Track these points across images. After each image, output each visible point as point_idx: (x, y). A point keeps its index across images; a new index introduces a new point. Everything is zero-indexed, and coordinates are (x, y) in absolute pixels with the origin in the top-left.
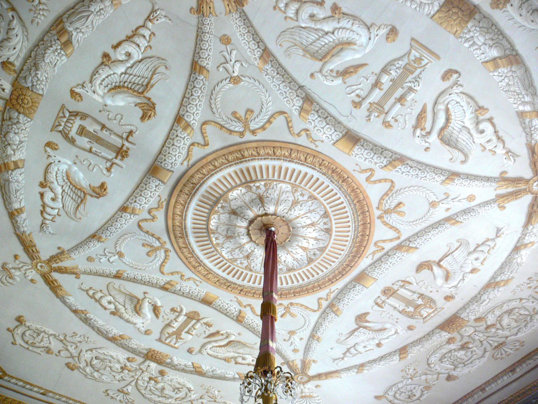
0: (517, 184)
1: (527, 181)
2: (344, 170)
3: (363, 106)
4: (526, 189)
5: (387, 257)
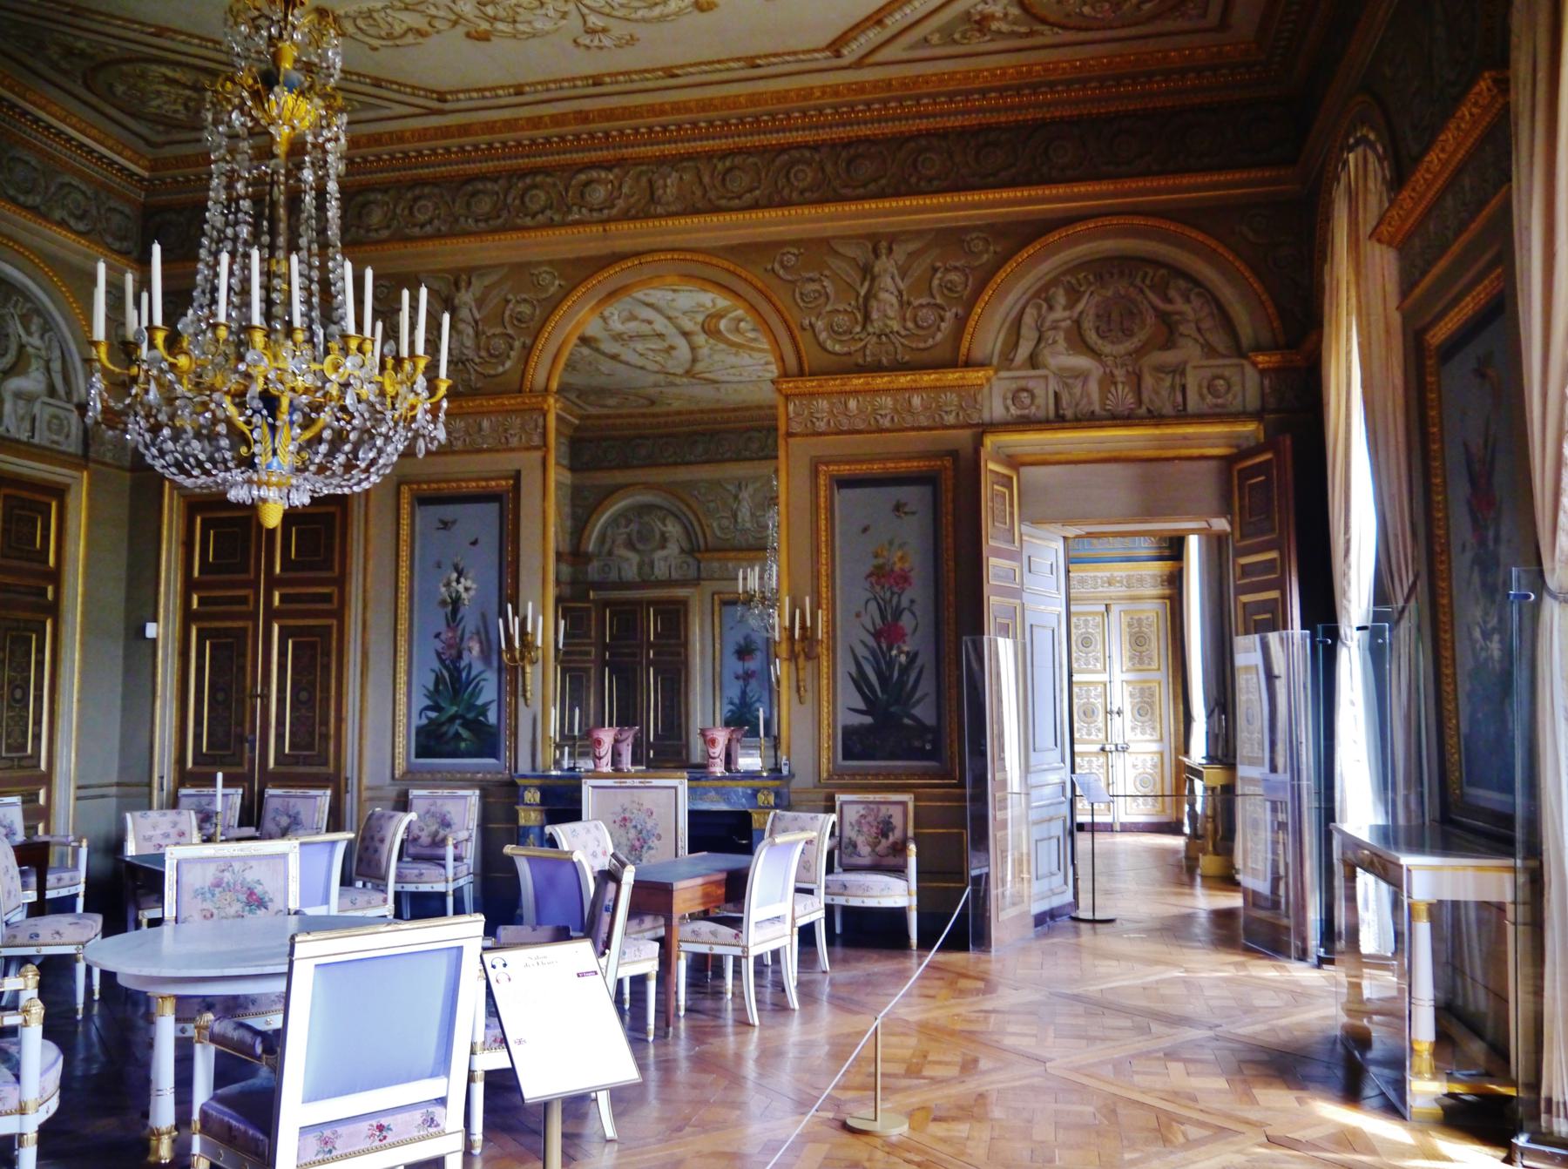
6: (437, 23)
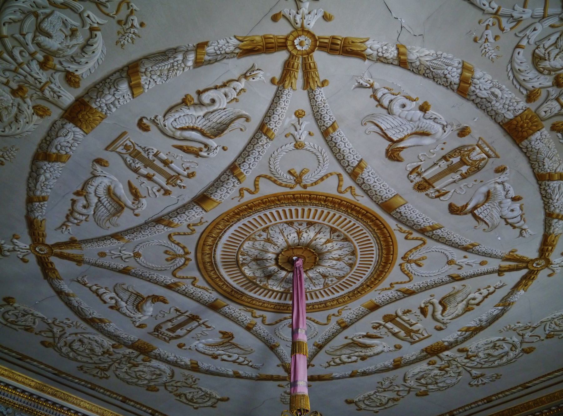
0: (293, 67)
1: (292, 56)
2: (237, 208)
3: (169, 189)
4: (304, 59)
6: (401, 393)
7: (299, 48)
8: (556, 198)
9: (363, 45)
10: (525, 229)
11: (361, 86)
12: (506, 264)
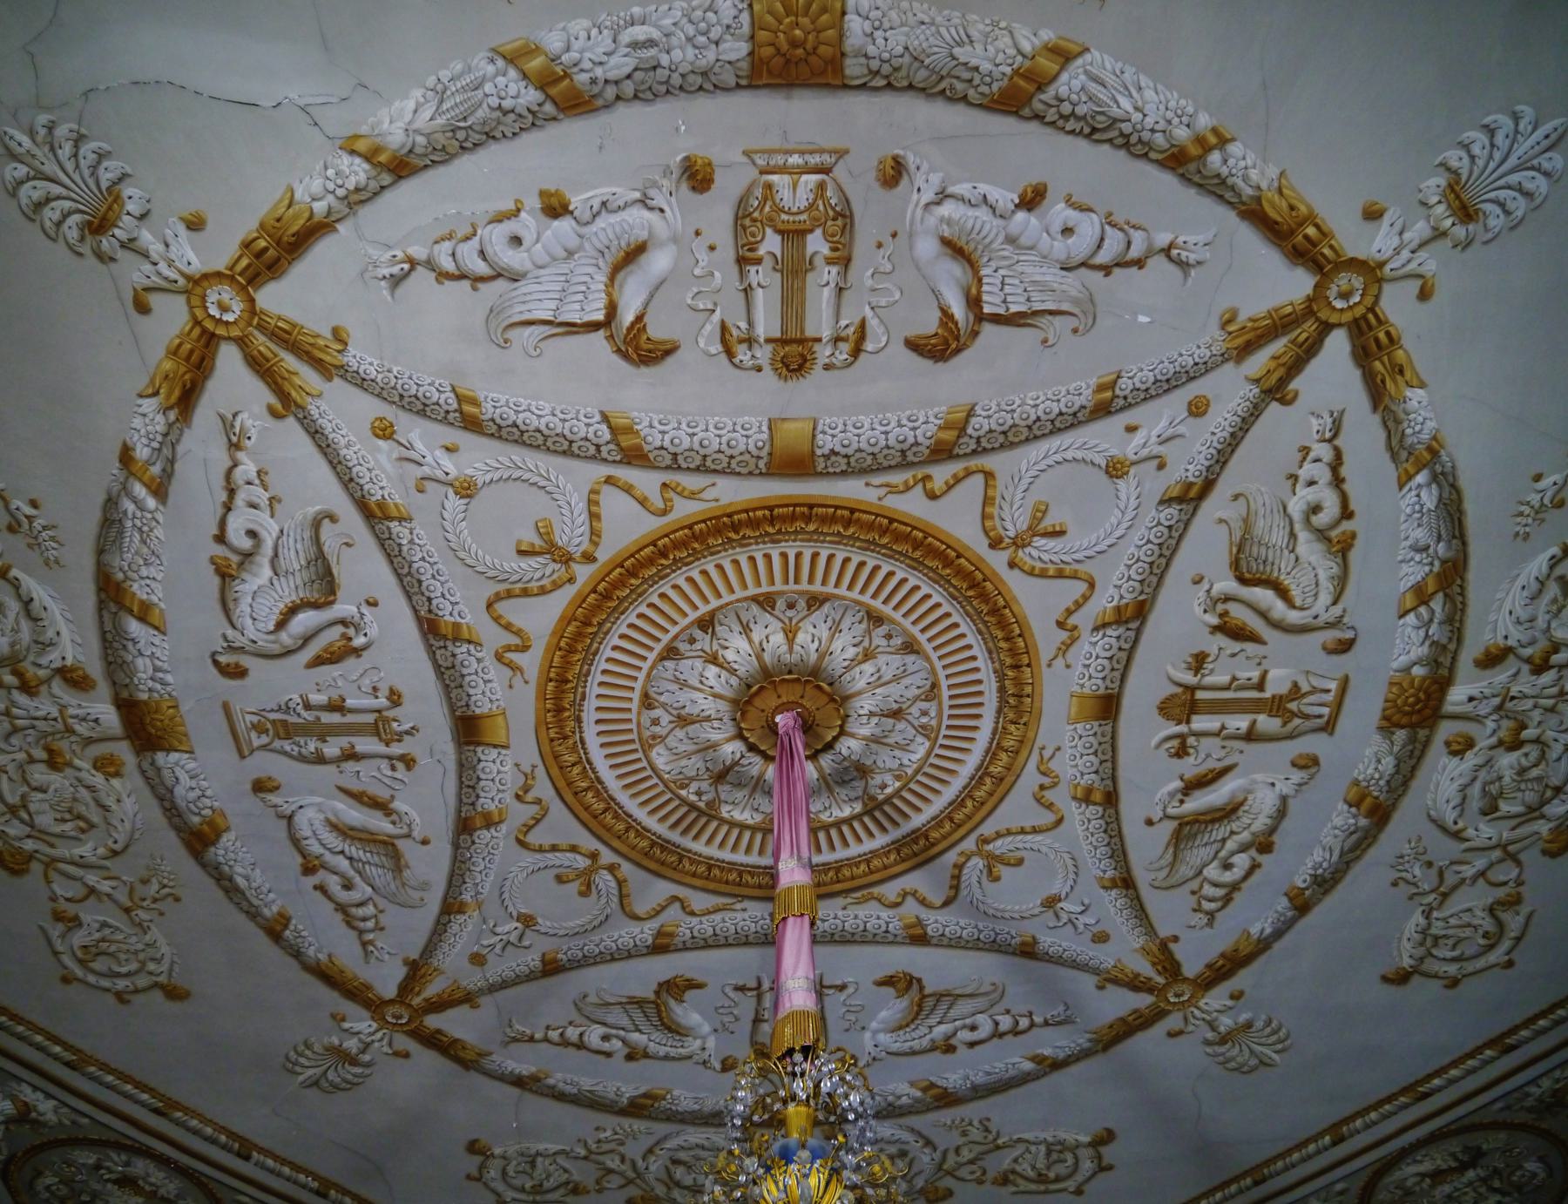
0: (268, 360)
1: (242, 342)
2: (542, 695)
4: (260, 327)
5: (680, 459)
7: (229, 317)
8: (1130, 109)
9: (296, 207)
10: (1171, 246)
11: (396, 281)
12: (1260, 361)
